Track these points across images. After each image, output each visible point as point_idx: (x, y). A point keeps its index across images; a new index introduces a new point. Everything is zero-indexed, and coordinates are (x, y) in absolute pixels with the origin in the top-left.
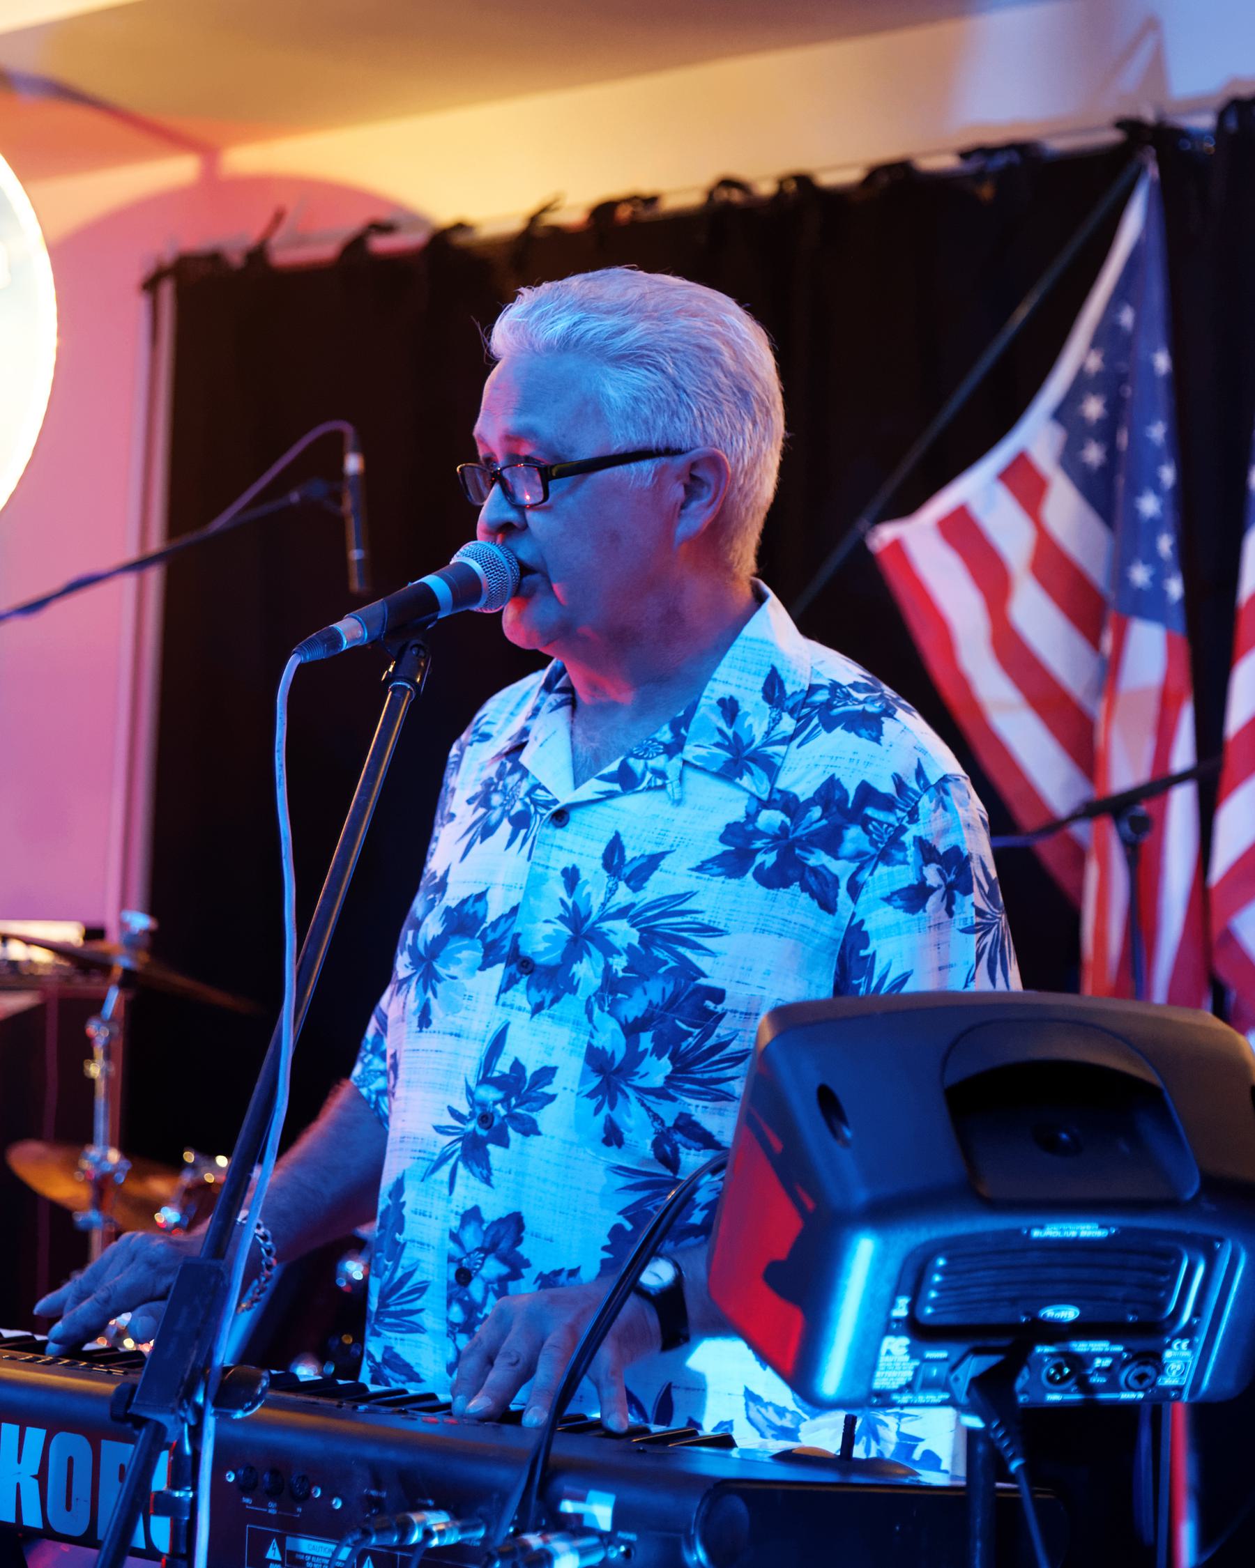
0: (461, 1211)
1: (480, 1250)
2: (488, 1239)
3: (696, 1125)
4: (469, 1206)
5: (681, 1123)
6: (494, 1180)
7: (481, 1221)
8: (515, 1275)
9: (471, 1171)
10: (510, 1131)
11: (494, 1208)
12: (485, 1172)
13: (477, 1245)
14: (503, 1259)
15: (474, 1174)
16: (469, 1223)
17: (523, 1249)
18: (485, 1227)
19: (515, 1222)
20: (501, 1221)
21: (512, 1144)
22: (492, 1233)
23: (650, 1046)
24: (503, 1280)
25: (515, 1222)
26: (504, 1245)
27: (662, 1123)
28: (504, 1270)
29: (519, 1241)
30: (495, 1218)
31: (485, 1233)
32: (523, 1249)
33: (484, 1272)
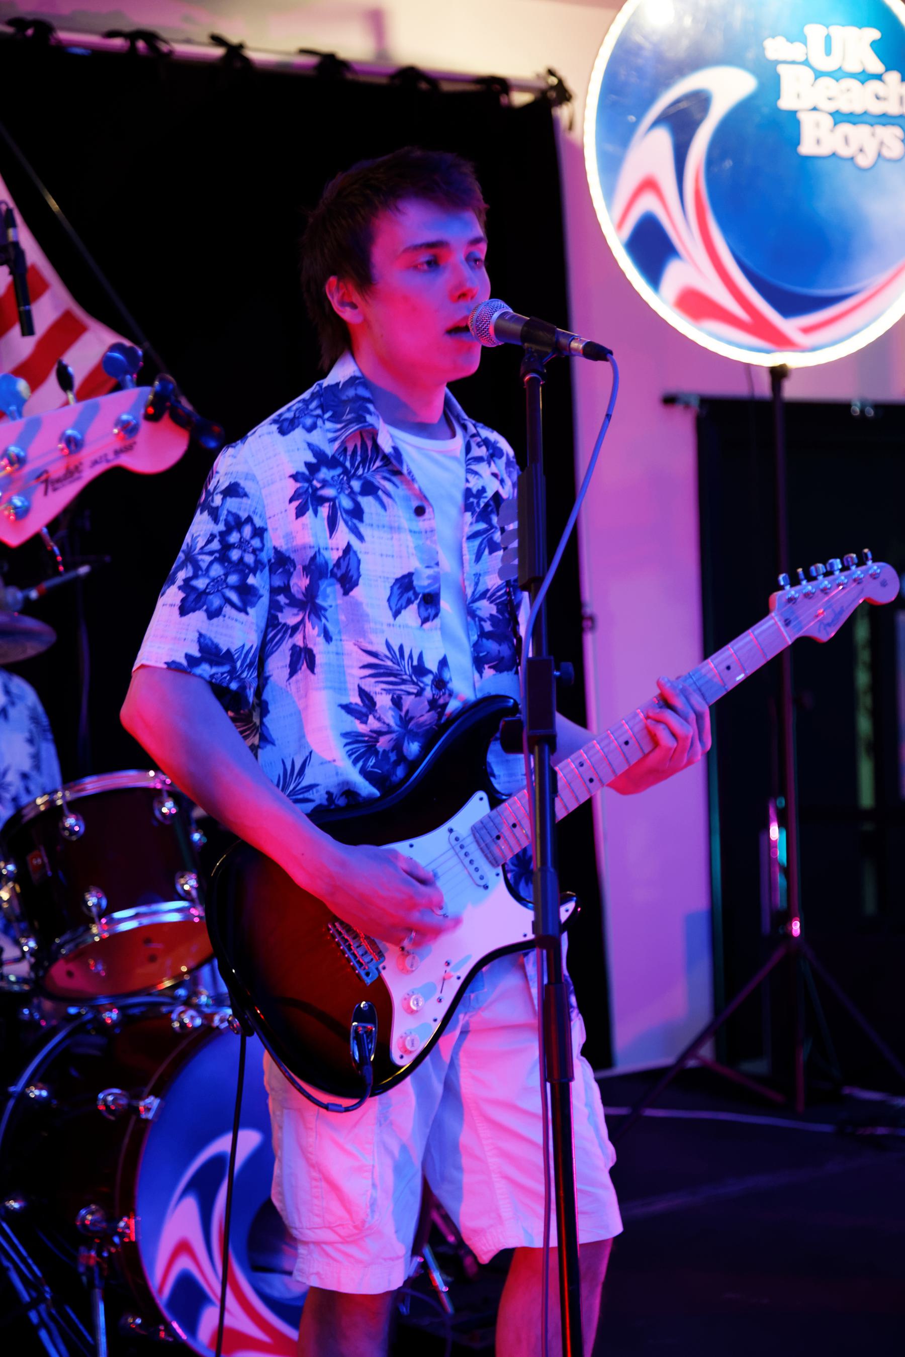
0: (221, 618)
1: (209, 594)
2: (203, 600)
3: (357, 718)
4: (215, 620)
5: (365, 718)
6: (197, 635)
7: (207, 611)
11: (198, 618)
12: (202, 640)
13: (211, 597)
16: (216, 610)
18: (205, 607)
22: (201, 604)
23: (390, 755)
27: (374, 717)
30: (197, 613)
33: (207, 581)
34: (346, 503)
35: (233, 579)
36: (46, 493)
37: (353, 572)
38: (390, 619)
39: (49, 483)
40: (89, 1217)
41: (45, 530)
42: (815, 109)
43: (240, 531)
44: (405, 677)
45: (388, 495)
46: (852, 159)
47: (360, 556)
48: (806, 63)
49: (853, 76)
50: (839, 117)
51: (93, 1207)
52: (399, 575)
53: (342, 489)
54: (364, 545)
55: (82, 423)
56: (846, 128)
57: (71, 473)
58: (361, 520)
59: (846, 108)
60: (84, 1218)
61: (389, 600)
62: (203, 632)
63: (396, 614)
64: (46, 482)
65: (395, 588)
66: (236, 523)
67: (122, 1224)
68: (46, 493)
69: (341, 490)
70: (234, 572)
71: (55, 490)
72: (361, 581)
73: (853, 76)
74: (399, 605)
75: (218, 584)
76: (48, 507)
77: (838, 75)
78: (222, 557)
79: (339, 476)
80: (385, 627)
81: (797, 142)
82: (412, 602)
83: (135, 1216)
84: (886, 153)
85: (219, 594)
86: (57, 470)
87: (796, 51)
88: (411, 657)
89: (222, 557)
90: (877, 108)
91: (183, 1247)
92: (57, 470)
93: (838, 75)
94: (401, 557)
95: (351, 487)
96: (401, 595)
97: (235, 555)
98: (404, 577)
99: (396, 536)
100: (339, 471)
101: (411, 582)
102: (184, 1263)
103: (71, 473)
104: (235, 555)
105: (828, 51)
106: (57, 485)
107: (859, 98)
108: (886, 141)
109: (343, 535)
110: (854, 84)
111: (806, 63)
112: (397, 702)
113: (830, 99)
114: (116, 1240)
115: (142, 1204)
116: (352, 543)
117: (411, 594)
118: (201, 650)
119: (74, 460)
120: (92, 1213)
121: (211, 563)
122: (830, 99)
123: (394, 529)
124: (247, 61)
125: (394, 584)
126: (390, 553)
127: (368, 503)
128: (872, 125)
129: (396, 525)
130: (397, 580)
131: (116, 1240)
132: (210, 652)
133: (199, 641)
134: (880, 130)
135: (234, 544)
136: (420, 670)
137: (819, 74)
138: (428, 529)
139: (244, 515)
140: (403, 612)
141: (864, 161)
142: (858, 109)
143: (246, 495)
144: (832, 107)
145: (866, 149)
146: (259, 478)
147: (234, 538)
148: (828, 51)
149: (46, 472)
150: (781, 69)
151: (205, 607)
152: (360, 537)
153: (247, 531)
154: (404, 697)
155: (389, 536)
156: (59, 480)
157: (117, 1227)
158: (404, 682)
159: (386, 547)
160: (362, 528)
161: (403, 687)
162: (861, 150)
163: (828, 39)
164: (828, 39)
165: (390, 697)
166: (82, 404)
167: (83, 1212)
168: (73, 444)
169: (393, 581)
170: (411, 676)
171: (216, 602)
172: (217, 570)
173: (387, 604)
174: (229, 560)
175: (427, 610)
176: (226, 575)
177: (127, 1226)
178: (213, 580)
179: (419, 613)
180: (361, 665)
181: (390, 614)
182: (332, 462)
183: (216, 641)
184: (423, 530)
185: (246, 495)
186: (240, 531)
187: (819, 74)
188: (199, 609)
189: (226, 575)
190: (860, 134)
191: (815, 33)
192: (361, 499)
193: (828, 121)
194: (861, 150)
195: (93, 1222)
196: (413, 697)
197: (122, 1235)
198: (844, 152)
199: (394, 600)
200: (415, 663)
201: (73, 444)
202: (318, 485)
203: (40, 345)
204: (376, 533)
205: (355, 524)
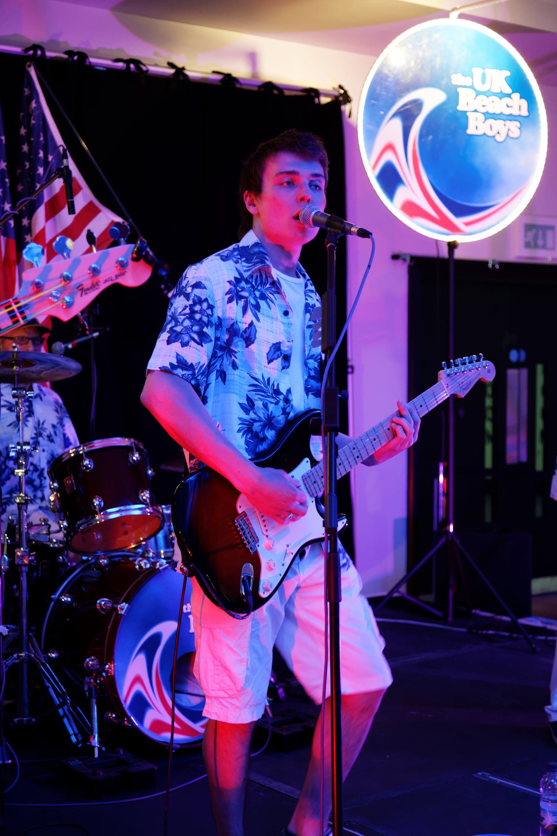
1: (183, 334)
6: (176, 354)
7: (181, 342)
8: (171, 328)
11: (176, 346)
13: (183, 335)
14: (175, 331)
17: (168, 335)
18: (180, 341)
19: (169, 342)
20: (174, 342)
24: (176, 325)
25: (169, 342)
26: (174, 335)
28: (175, 329)
29: (169, 337)
30: (176, 343)
31: (180, 339)
32: (168, 335)
33: (182, 328)
34: (253, 301)
35: (196, 328)
36: (81, 295)
37: (252, 336)
39: (83, 290)
40: (91, 663)
41: (80, 314)
42: (476, 111)
46: (494, 136)
48: (472, 87)
49: (495, 94)
50: (488, 116)
51: (93, 657)
55: (101, 261)
56: (491, 121)
57: (94, 286)
59: (491, 111)
60: (88, 663)
61: (267, 354)
62: (179, 353)
63: (270, 362)
64: (82, 290)
65: (272, 348)
67: (107, 666)
68: (81, 295)
70: (196, 325)
71: (86, 294)
72: (256, 341)
73: (495, 94)
75: (188, 330)
76: (82, 302)
77: (488, 94)
78: (191, 317)
81: (467, 128)
83: (114, 663)
84: (511, 135)
86: (87, 284)
87: (467, 81)
89: (191, 317)
90: (507, 111)
91: (138, 679)
92: (87, 284)
93: (488, 94)
96: (275, 352)
102: (138, 687)
103: (94, 286)
105: (483, 82)
106: (87, 292)
107: (498, 106)
108: (511, 129)
109: (250, 317)
110: (496, 99)
111: (472, 87)
113: (483, 106)
114: (104, 674)
115: (118, 655)
116: (254, 321)
118: (177, 362)
119: (95, 280)
120: (92, 660)
121: (184, 319)
122: (483, 106)
124: (186, 76)
125: (272, 346)
128: (504, 121)
131: (104, 674)
134: (508, 123)
137: (478, 93)
140: (275, 361)
141: (499, 138)
142: (498, 112)
144: (484, 110)
145: (501, 132)
148: (483, 82)
149: (82, 285)
150: (460, 90)
151: (180, 341)
152: (258, 319)
156: (88, 289)
157: (105, 668)
162: (498, 133)
163: (484, 75)
164: (484, 75)
166: (100, 252)
167: (88, 660)
168: (95, 272)
171: (186, 338)
172: (187, 323)
173: (266, 356)
176: (192, 326)
177: (110, 668)
178: (185, 327)
181: (266, 361)
187: (478, 93)
188: (177, 341)
189: (192, 326)
190: (498, 125)
191: (477, 72)
193: (482, 117)
194: (498, 133)
195: (92, 665)
197: (107, 672)
198: (490, 133)
199: (271, 354)
201: (95, 272)
202: (240, 290)
203: (76, 218)
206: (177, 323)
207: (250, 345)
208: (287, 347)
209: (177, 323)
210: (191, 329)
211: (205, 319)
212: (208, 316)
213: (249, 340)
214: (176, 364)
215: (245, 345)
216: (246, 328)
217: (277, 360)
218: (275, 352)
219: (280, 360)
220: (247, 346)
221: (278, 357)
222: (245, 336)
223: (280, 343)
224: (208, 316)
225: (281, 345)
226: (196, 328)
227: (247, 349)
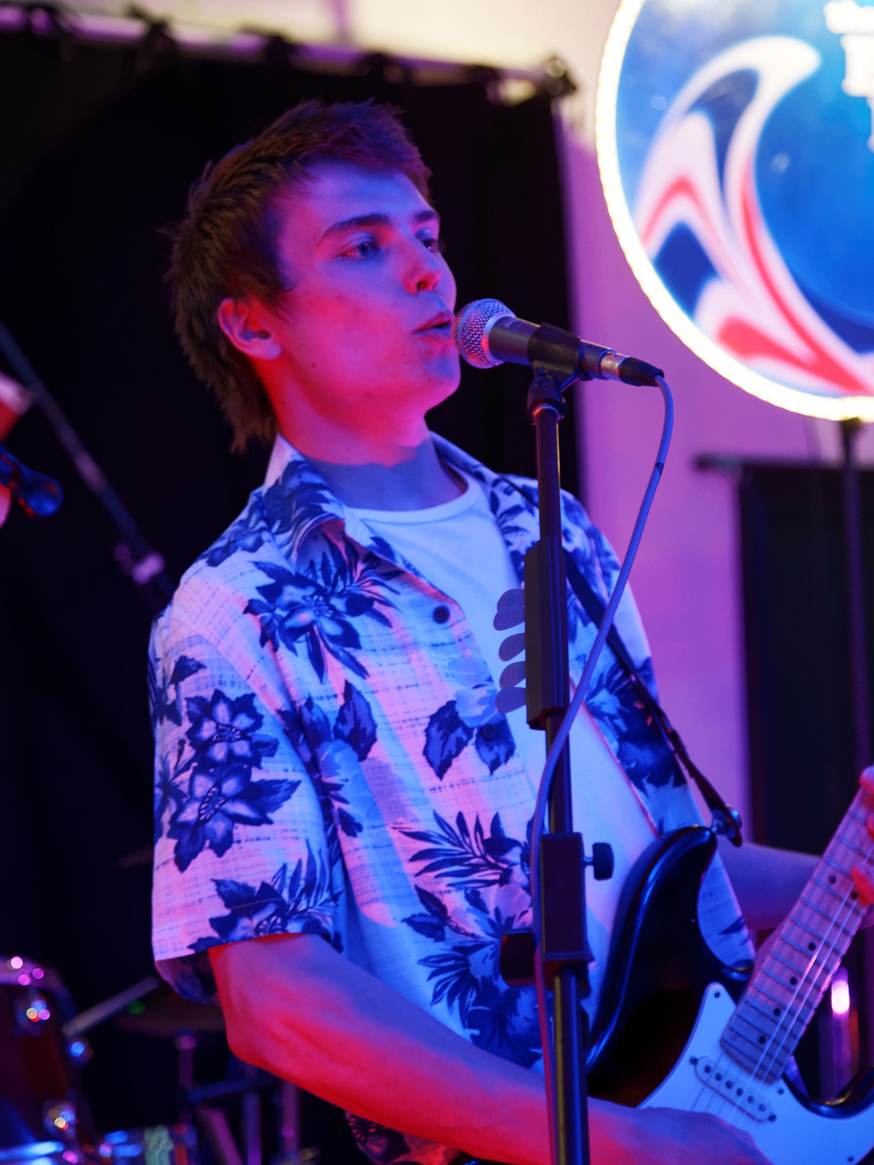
0: (235, 846)
9: (237, 884)
10: (215, 934)
12: (223, 889)
15: (233, 882)
21: (208, 924)
35: (230, 786)
38: (436, 781)
43: (212, 718)
44: (474, 861)
45: (386, 603)
47: (368, 697)
52: (433, 711)
53: (320, 611)
54: (369, 681)
58: (357, 646)
61: (426, 752)
62: (219, 877)
63: (441, 770)
65: (434, 730)
66: (203, 709)
69: (320, 614)
70: (227, 777)
74: (446, 753)
75: (214, 800)
78: (203, 763)
79: (312, 596)
80: (428, 794)
82: (465, 744)
85: (219, 814)
88: (478, 827)
94: (430, 683)
95: (332, 607)
96: (445, 738)
97: (219, 752)
98: (442, 710)
99: (414, 656)
100: (310, 591)
101: (455, 715)
104: (219, 752)
112: (475, 901)
117: (459, 732)
118: (227, 905)
123: (406, 647)
125: (431, 724)
126: (413, 682)
127: (362, 624)
129: (410, 639)
130: (433, 718)
132: (240, 900)
133: (220, 894)
135: (211, 738)
136: (498, 843)
138: (463, 636)
139: (208, 694)
140: (455, 762)
143: (200, 666)
146: (206, 636)
147: (208, 730)
153: (222, 712)
154: (481, 890)
155: (404, 659)
158: (475, 869)
159: (406, 676)
160: (362, 657)
161: (475, 876)
165: (461, 894)
169: (427, 721)
170: (483, 857)
174: (214, 763)
175: (491, 749)
176: (218, 785)
179: (481, 756)
180: (410, 857)
181: (431, 772)
182: (300, 581)
183: (241, 881)
184: (456, 639)
185: (200, 666)
186: (212, 718)
189: (218, 785)
192: (349, 619)
196: (496, 887)
199: (436, 747)
200: (487, 835)
204: (384, 659)
205: (348, 654)
206: (182, 799)
207: (368, 749)
208: (481, 702)
209: (182, 799)
210: (220, 793)
211: (242, 748)
212: (245, 735)
213: (360, 737)
214: (226, 912)
215: (355, 756)
216: (342, 708)
217: (462, 755)
218: (445, 738)
219: (470, 750)
220: (363, 756)
221: (461, 745)
222: (346, 730)
223: (451, 705)
224: (245, 735)
225: (458, 708)
226: (230, 786)
227: (364, 764)
